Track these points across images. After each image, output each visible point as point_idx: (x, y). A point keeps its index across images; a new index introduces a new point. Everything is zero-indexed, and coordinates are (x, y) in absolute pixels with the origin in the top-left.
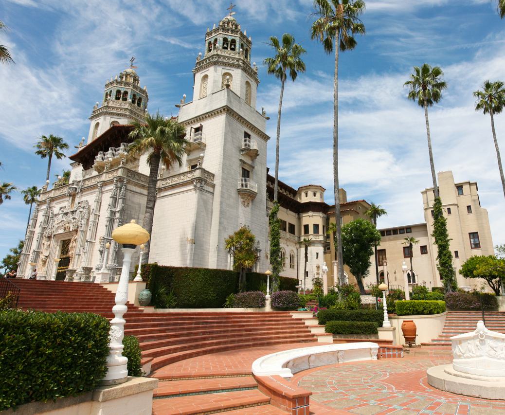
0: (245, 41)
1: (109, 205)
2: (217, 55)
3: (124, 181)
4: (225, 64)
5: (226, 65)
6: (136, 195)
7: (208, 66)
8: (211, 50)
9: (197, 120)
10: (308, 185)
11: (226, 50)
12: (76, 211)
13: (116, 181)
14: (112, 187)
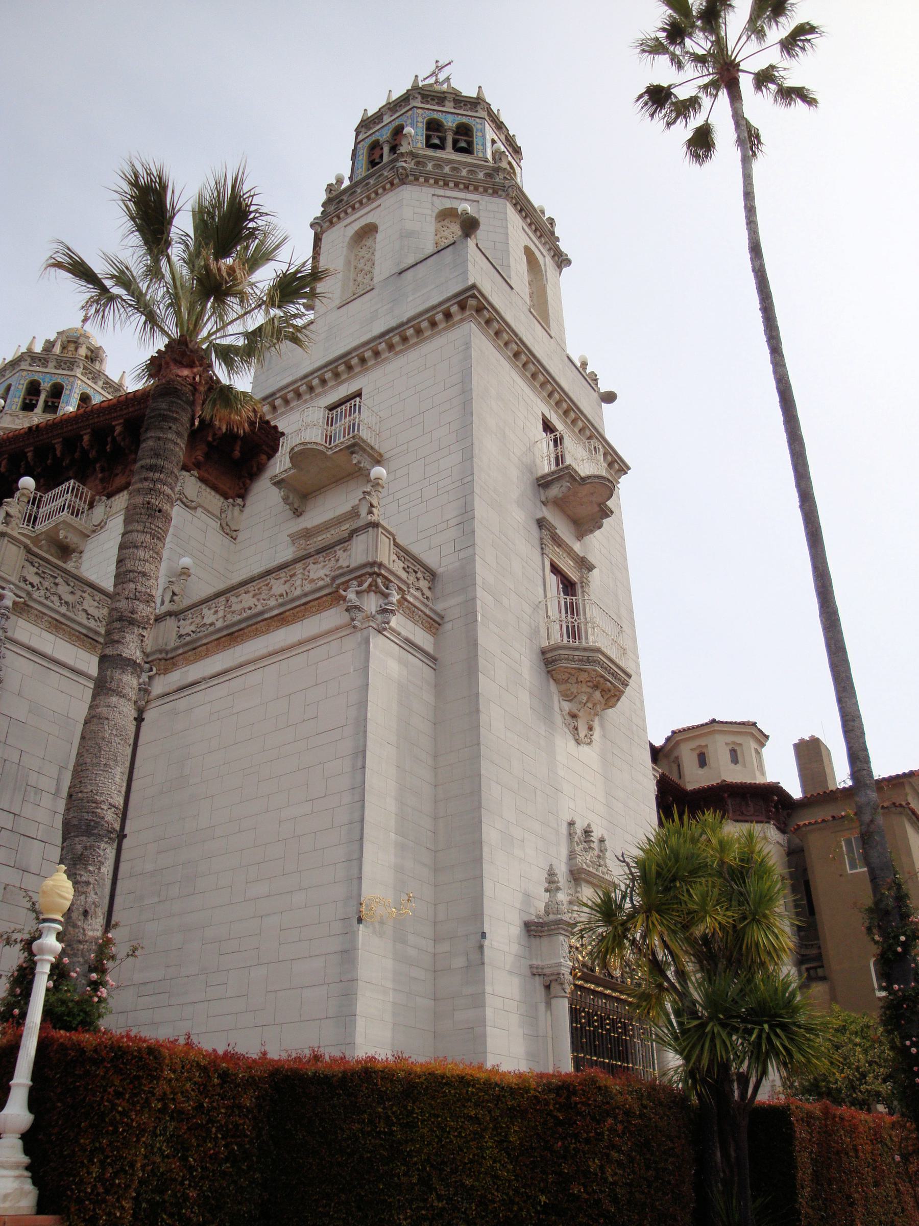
6: (54, 678)
9: (337, 375)
10: (707, 721)
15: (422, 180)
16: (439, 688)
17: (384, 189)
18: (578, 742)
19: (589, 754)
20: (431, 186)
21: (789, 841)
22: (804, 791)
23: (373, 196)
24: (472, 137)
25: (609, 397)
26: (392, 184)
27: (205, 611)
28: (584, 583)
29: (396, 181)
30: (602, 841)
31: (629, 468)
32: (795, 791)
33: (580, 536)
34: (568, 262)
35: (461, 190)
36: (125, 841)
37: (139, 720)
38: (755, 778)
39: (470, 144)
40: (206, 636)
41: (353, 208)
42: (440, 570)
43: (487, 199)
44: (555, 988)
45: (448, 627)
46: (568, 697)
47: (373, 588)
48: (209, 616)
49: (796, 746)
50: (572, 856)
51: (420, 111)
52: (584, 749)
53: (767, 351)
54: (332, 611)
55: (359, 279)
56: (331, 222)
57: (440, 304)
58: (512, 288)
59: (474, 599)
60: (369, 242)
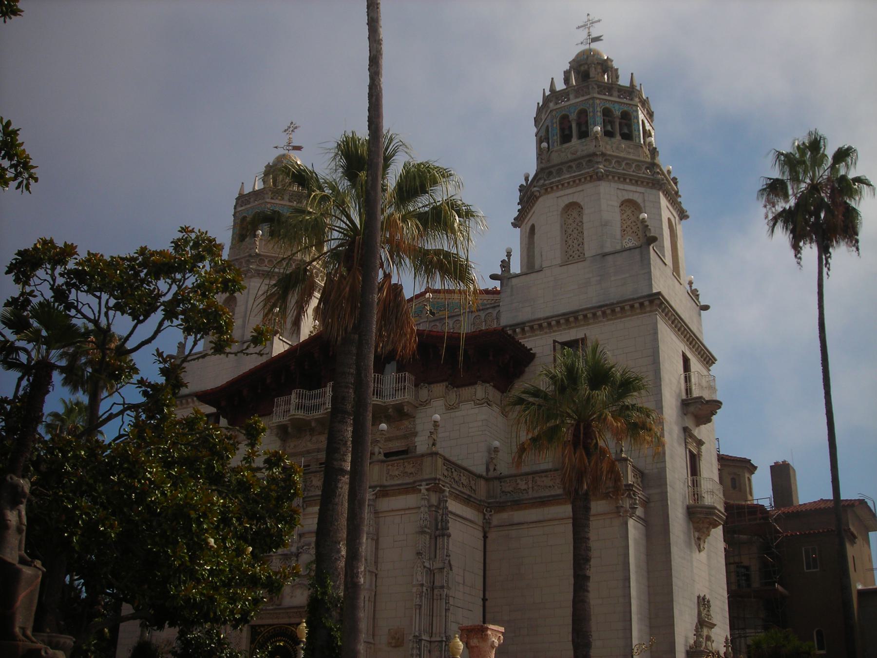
1: (419, 554)
2: (603, 154)
4: (623, 178)
5: (625, 179)
7: (577, 181)
11: (613, 140)
12: (297, 555)
13: (427, 490)
14: (411, 500)
15: (610, 177)
17: (585, 178)
19: (703, 554)
20: (615, 182)
23: (577, 181)
24: (630, 120)
25: (706, 308)
26: (591, 177)
27: (519, 481)
29: (595, 177)
30: (708, 601)
31: (716, 360)
33: (698, 424)
34: (687, 217)
35: (633, 184)
36: (487, 603)
37: (485, 537)
38: (746, 500)
39: (631, 132)
40: (526, 499)
41: (563, 185)
42: (646, 471)
43: (649, 190)
46: (697, 529)
47: (629, 496)
48: (522, 485)
51: (598, 102)
52: (702, 553)
53: (823, 391)
54: (604, 502)
55: (570, 242)
56: (546, 190)
57: (638, 298)
59: (666, 492)
60: (575, 214)
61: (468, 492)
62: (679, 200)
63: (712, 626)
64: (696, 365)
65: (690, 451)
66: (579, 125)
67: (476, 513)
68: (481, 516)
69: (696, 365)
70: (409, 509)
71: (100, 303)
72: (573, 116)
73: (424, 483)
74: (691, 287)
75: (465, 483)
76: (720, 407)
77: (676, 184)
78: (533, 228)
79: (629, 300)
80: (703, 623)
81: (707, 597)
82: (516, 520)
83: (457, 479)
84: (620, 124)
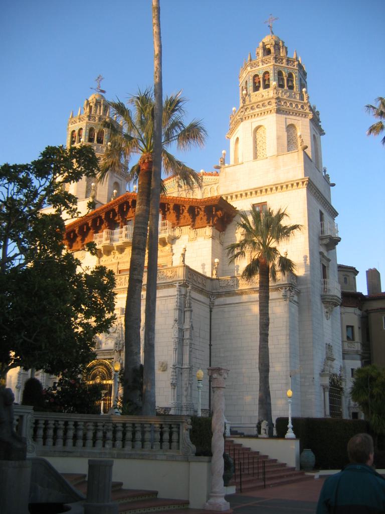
0: (302, 73)
3: (188, 287)
8: (259, 87)
16: (300, 311)
18: (327, 319)
21: (363, 313)
22: (369, 291)
25: (333, 185)
28: (328, 266)
29: (273, 111)
31: (338, 214)
32: (365, 293)
37: (211, 311)
43: (303, 119)
44: (326, 390)
45: (302, 294)
46: (326, 307)
47: (289, 290)
49: (367, 272)
50: (327, 354)
58: (312, 161)
61: (202, 287)
62: (320, 124)
63: (333, 360)
64: (326, 216)
65: (323, 265)
66: (264, 81)
67: (206, 298)
68: (209, 299)
69: (326, 216)
70: (170, 296)
71: (8, 192)
72: (261, 76)
73: (177, 282)
74: (325, 173)
75: (200, 282)
76: (340, 241)
77: (319, 114)
78: (238, 139)
79: (291, 181)
80: (329, 358)
81: (331, 344)
82: (228, 303)
83: (196, 280)
84: (288, 81)
